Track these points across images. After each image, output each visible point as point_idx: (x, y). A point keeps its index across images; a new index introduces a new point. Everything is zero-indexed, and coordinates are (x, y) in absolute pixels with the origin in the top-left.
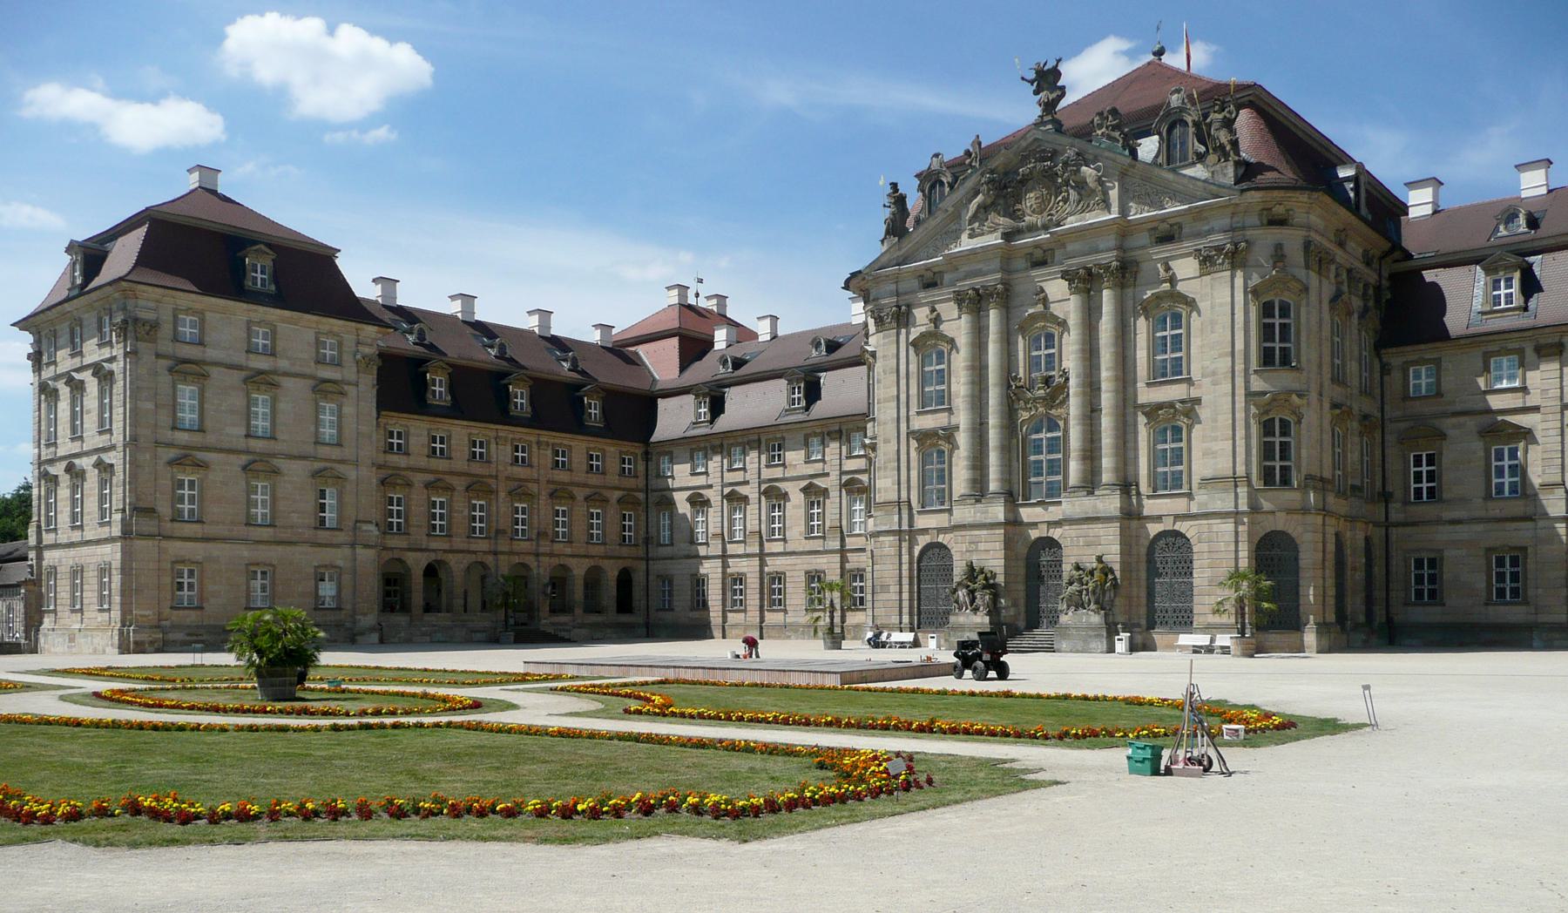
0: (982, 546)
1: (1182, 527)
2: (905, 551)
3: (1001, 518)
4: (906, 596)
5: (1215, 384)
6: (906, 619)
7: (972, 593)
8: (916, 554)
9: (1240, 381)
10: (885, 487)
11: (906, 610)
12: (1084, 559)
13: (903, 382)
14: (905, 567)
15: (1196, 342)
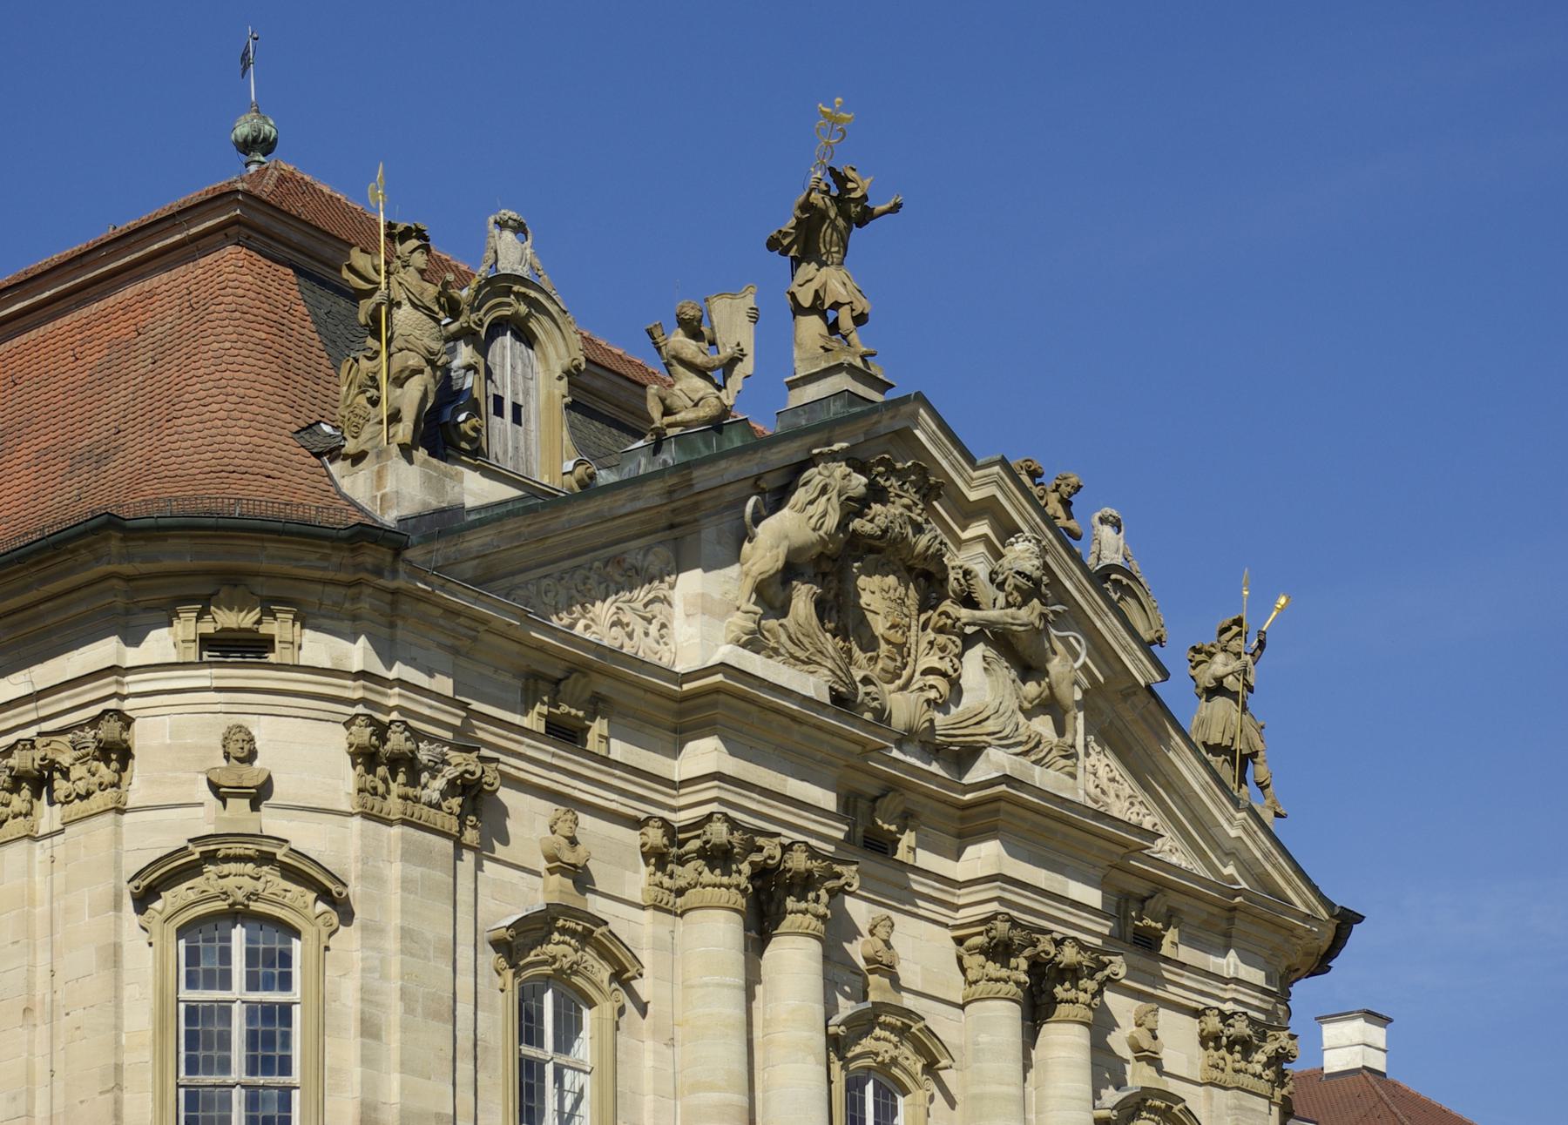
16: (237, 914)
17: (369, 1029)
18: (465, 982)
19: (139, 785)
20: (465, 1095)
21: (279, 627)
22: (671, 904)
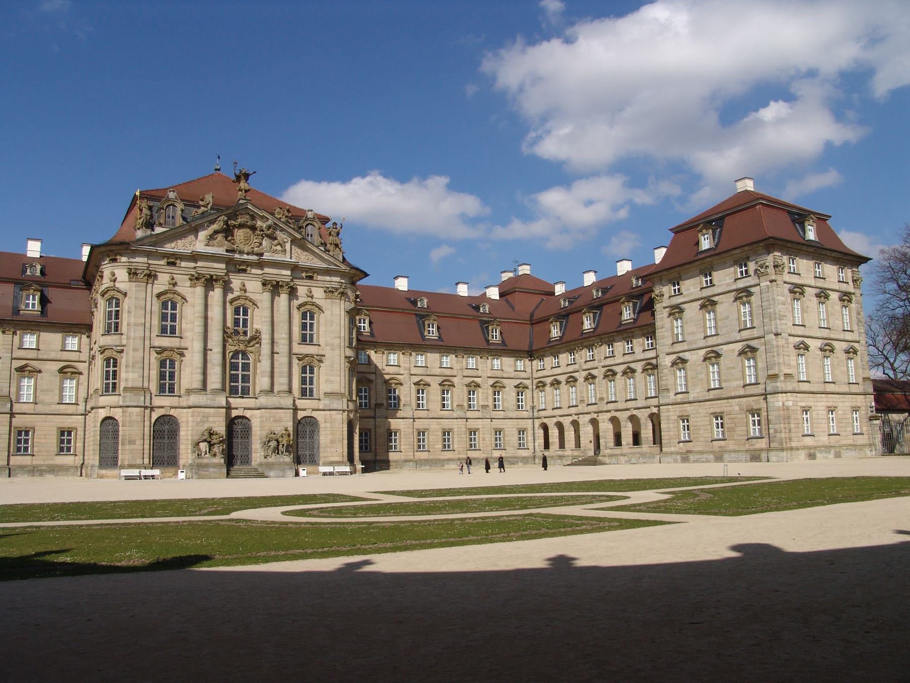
0: (211, 419)
1: (315, 414)
2: (147, 419)
3: (224, 404)
4: (147, 447)
5: (333, 349)
6: (146, 461)
7: (211, 445)
8: (153, 421)
9: (342, 350)
10: (128, 376)
11: (146, 456)
12: (273, 429)
13: (148, 316)
14: (147, 429)
15: (322, 329)
16: (112, 298)
17: (129, 312)
18: (149, 303)
19: (104, 281)
20: (148, 319)
21: (118, 257)
22: (193, 286)
